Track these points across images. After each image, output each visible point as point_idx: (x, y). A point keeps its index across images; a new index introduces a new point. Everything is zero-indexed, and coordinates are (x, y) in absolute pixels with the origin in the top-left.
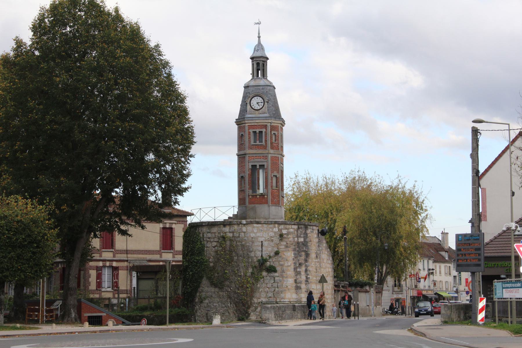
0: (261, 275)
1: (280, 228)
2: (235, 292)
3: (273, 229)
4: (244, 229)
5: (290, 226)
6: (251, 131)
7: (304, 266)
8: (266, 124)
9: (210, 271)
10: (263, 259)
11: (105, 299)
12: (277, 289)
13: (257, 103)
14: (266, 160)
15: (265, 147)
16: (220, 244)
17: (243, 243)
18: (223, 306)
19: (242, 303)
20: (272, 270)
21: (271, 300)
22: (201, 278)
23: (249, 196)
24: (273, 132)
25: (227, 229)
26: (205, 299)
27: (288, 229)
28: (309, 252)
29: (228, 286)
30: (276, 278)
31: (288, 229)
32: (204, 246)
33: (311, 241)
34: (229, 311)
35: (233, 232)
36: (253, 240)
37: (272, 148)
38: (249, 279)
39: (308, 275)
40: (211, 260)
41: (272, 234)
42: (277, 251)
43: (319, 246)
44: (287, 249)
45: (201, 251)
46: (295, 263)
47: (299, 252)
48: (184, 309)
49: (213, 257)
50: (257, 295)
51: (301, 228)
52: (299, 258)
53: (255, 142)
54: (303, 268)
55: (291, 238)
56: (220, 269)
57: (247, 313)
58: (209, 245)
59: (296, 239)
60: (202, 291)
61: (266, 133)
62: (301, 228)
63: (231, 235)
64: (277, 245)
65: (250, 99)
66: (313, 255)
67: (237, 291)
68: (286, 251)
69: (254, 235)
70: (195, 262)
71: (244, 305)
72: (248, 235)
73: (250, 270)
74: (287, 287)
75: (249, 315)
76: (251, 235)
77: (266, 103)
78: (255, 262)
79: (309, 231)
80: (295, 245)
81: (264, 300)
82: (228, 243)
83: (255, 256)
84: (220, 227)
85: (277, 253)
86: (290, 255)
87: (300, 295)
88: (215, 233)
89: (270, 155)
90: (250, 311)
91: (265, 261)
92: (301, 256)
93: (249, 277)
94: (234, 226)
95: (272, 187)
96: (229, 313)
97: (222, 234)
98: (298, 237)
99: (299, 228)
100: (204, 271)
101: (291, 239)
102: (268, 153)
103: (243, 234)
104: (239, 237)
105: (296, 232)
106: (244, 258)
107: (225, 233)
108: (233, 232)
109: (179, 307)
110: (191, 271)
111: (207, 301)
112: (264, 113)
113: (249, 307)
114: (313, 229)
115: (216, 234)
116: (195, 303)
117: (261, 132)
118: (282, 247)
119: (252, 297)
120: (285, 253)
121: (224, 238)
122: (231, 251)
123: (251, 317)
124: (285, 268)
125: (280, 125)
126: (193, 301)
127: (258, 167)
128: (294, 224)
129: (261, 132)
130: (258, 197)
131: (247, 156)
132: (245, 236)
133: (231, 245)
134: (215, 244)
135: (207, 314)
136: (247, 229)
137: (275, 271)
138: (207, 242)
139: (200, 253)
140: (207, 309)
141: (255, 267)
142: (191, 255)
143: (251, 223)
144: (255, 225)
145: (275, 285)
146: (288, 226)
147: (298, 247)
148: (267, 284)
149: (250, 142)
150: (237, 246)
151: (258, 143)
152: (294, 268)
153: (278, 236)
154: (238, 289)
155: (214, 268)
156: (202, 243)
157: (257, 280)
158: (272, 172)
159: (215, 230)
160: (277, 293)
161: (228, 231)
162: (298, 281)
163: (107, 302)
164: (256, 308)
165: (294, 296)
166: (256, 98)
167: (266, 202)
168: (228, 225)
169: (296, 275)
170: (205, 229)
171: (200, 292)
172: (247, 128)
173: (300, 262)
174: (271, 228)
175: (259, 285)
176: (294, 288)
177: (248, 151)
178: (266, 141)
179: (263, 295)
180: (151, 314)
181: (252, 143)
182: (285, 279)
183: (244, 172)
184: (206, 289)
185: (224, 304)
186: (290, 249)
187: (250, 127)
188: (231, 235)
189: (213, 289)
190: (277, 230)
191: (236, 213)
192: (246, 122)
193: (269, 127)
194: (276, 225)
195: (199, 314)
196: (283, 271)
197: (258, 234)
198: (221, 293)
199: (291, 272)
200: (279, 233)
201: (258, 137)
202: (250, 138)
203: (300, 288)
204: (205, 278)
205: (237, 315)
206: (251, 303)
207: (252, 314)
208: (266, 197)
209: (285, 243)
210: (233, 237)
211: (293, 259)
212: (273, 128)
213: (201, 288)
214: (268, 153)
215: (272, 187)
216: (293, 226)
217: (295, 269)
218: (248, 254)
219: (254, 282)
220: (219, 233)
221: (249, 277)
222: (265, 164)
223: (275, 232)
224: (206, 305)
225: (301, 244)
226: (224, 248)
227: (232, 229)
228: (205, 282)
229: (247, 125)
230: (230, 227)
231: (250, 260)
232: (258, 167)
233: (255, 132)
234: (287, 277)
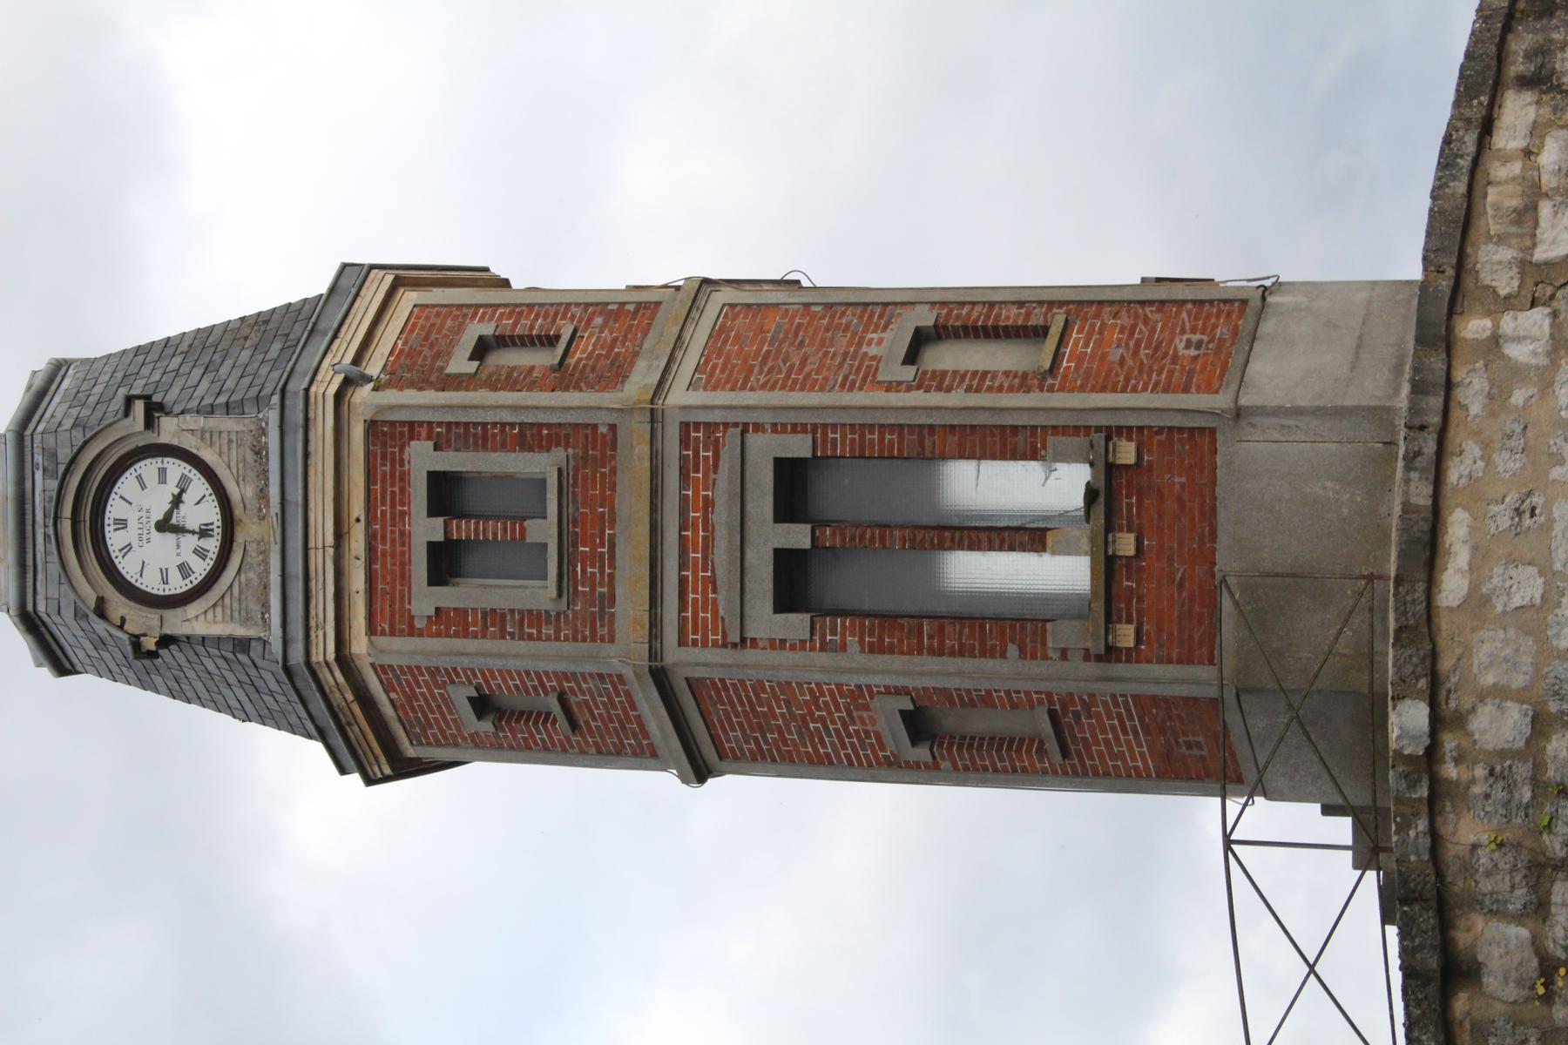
1: (1506, 283)
3: (1518, 373)
4: (1498, 726)
5: (1504, 172)
6: (424, 600)
8: (357, 433)
13: (164, 526)
14: (732, 438)
15: (592, 446)
23: (1111, 653)
24: (460, 363)
27: (1534, 194)
31: (1534, 194)
37: (616, 373)
51: (1541, 52)
53: (529, 562)
61: (447, 435)
62: (1541, 52)
65: (119, 606)
77: (168, 430)
89: (679, 396)
95: (1022, 382)
99: (1539, 80)
102: (654, 418)
112: (260, 452)
117: (446, 493)
125: (408, 299)
127: (798, 536)
128: (1487, 127)
129: (446, 493)
130: (1126, 544)
131: (673, 654)
136: (1501, 693)
143: (1421, 629)
144: (1453, 586)
146: (1500, 196)
149: (530, 622)
151: (543, 530)
158: (868, 376)
161: (1519, 933)
166: (115, 540)
167: (1197, 442)
168: (1445, 924)
172: (400, 650)
174: (1497, 397)
177: (624, 653)
178: (531, 437)
181: (541, 594)
183: (858, 697)
187: (387, 614)
191: (1341, 829)
192: (325, 649)
193: (391, 397)
194: (1474, 327)
201: (494, 529)
202: (495, 621)
208: (1126, 453)
212: (417, 366)
214: (654, 418)
215: (1022, 382)
222: (765, 449)
227: (1497, 878)
229: (360, 644)
230: (1475, 902)
232: (798, 536)
233: (446, 563)
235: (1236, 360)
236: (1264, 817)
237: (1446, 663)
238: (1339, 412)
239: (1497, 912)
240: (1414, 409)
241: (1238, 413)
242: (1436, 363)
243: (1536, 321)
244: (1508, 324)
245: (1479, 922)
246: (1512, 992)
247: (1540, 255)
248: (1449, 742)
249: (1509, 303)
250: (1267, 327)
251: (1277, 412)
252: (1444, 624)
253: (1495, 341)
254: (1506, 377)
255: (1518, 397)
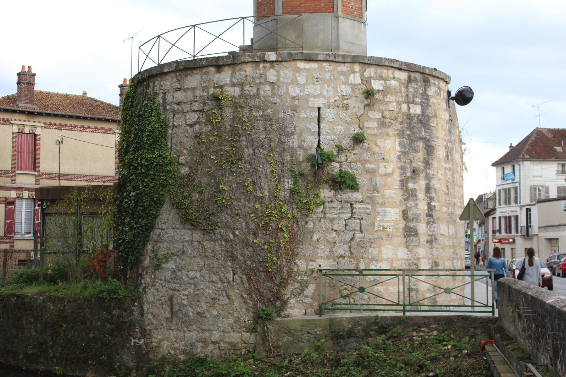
0: (317, 196)
1: (366, 74)
2: (246, 244)
3: (347, 77)
4: (272, 75)
5: (390, 73)
7: (422, 175)
9: (180, 186)
10: (322, 155)
11: (19, 251)
12: (358, 235)
16: (208, 116)
17: (269, 111)
18: (215, 278)
19: (267, 272)
20: (343, 183)
21: (347, 264)
22: (159, 203)
25: (225, 77)
26: (166, 258)
27: (385, 79)
28: (432, 143)
29: (227, 226)
30: (357, 206)
31: (385, 79)
32: (167, 126)
33: (435, 116)
34: (231, 293)
35: (241, 85)
36: (297, 103)
38: (285, 208)
39: (431, 199)
40: (182, 159)
41: (347, 90)
42: (358, 134)
43: (450, 131)
44: (384, 130)
45: (159, 138)
46: (403, 168)
47: (412, 140)
48: (115, 283)
49: (189, 151)
50: (306, 249)
51: (416, 80)
52: (411, 156)
54: (422, 183)
55: (393, 104)
56: (205, 181)
57: (278, 298)
58: (179, 121)
59: (404, 106)
60: (160, 239)
62: (416, 80)
63: (236, 91)
64: (359, 118)
66: (440, 153)
67: (251, 238)
68: (381, 135)
69: (298, 90)
70: (142, 166)
71: (270, 278)
72: (283, 91)
73: (288, 183)
74: (384, 228)
75: (285, 303)
76: (291, 90)
78: (300, 163)
79: (431, 91)
80: (401, 123)
81: (325, 265)
82: (228, 112)
83: (301, 147)
84: (207, 74)
85: (358, 140)
86: (390, 145)
87: (415, 250)
88: (194, 89)
90: (287, 293)
91: (329, 159)
92: (416, 151)
93: (284, 202)
94: (244, 66)
96: (228, 297)
97: (212, 91)
98: (409, 102)
99: (410, 80)
100: (164, 186)
101: (393, 106)
103: (268, 88)
104: (257, 95)
105: (403, 89)
106: (271, 151)
107: (221, 87)
108: (241, 85)
109: (105, 279)
110: (135, 188)
111: (170, 265)
113: (284, 284)
114: (439, 88)
115: (198, 93)
116: (143, 268)
118: (371, 126)
119: (292, 255)
120: (379, 142)
121: (216, 99)
122: (235, 134)
123: (288, 311)
124: (378, 180)
126: (137, 263)
128: (400, 69)
132: (274, 94)
133: (236, 118)
134: (193, 117)
135: (171, 299)
137: (354, 187)
138: (175, 113)
139: (155, 142)
140: (171, 285)
141: (302, 175)
142: (137, 149)
143: (292, 58)
145: (354, 223)
146: (385, 72)
147: (410, 127)
148: (332, 220)
150: (252, 119)
152: (402, 181)
153: (362, 97)
154: (255, 234)
155: (190, 178)
156: (162, 117)
157: (306, 209)
159: (194, 80)
160: (358, 244)
162: (410, 214)
163: (23, 256)
164: (304, 286)
165: (402, 253)
168: (229, 65)
169: (406, 200)
170: (168, 83)
171: (156, 242)
173: (414, 165)
174: (342, 73)
175: (310, 225)
176: (401, 232)
179: (323, 250)
180: (40, 294)
182: (379, 209)
184: (170, 231)
185: (216, 273)
186: (391, 131)
188: (236, 91)
189: (186, 234)
190: (360, 81)
191: (248, 43)
194: (357, 67)
195: (151, 299)
196: (375, 189)
197: (310, 89)
198: (208, 245)
199: (392, 191)
200: (364, 88)
203: (416, 234)
204: (166, 206)
205: (251, 304)
206: (290, 272)
207: (292, 301)
209: (378, 116)
210: (241, 96)
211: (399, 158)
213: (157, 231)
216: (398, 74)
217: (403, 183)
218: (281, 142)
219: (298, 215)
220: (205, 89)
221: (284, 202)
223: (353, 86)
224: (168, 275)
225: (415, 120)
226: (219, 127)
228: (167, 216)
231: (288, 157)
234: (383, 204)
235: (349, 16)
236: (250, 26)
237: (284, 64)
238: (338, 39)
239: (232, 76)
240: (339, 55)
241: (337, 17)
242: (349, 60)
243: (358, 81)
244: (358, 75)
245: (230, 72)
246: (215, 80)
247: (372, 81)
248: (268, 65)
249: (362, 75)
250: (356, 23)
251: (338, 26)
252: (293, 63)
253: (354, 72)
254: (346, 75)
255: (342, 77)
